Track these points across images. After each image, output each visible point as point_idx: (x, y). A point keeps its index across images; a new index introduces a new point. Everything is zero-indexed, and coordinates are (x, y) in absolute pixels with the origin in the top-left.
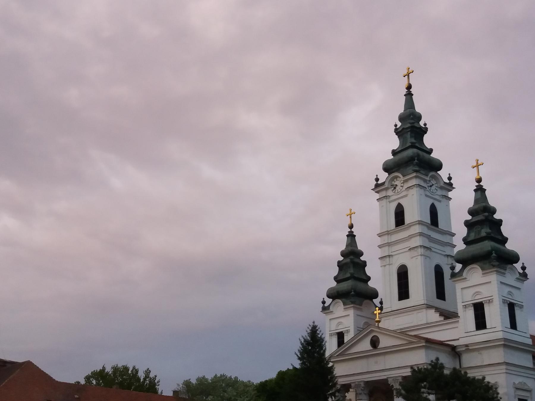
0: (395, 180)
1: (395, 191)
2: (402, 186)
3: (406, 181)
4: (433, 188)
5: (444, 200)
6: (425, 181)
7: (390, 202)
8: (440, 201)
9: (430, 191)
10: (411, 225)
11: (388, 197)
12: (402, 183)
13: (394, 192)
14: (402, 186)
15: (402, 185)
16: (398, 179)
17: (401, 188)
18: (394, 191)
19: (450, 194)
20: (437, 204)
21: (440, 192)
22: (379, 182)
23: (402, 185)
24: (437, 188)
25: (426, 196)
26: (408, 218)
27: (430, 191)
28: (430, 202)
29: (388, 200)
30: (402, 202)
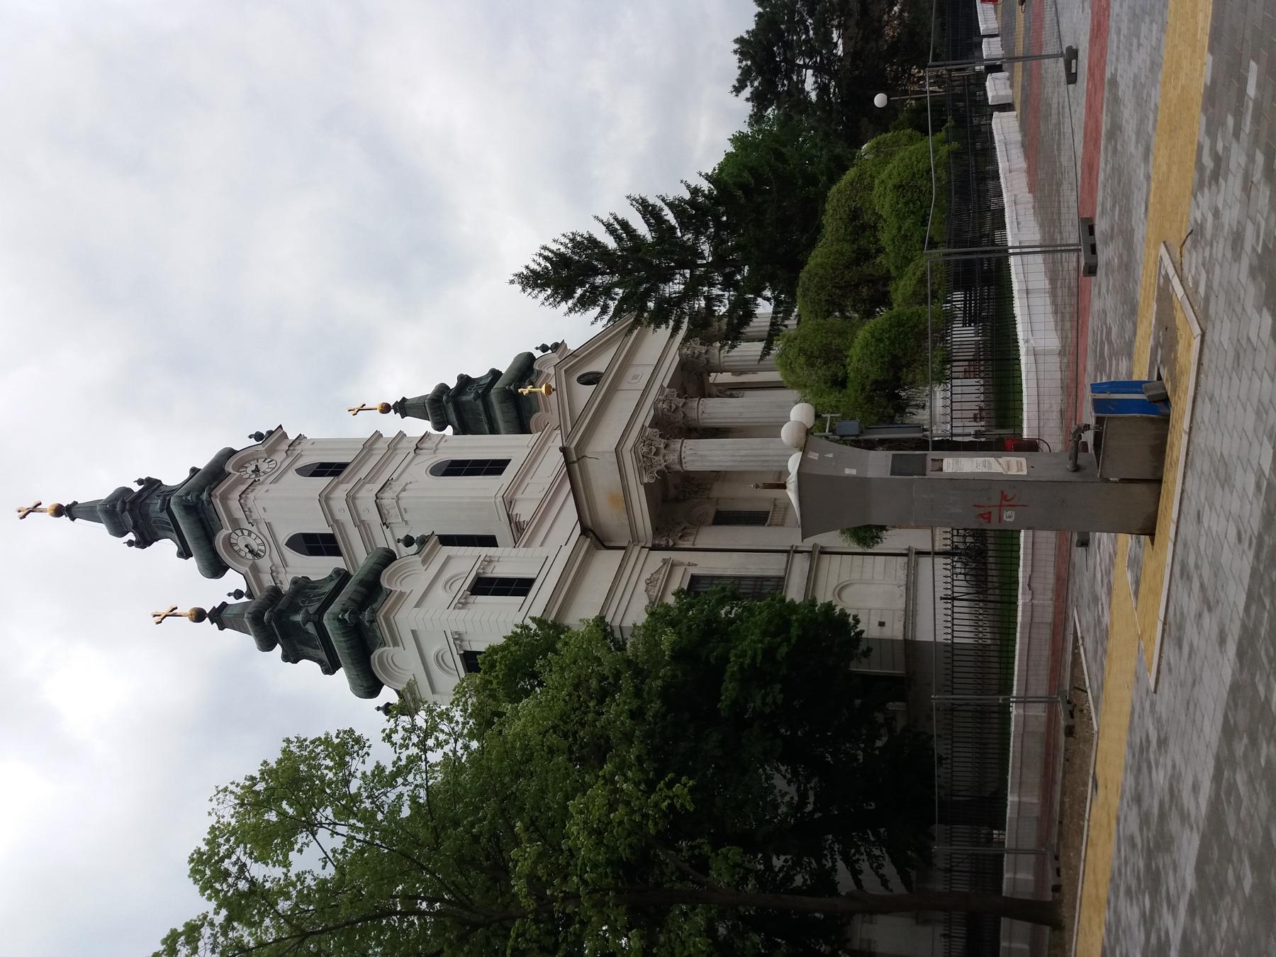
0: (236, 548)
1: (260, 550)
2: (249, 535)
3: (235, 523)
4: (264, 467)
5: (299, 448)
6: (240, 481)
7: (285, 564)
8: (299, 456)
11: (273, 568)
13: (263, 554)
15: (246, 533)
16: (233, 541)
17: (253, 535)
18: (263, 554)
19: (292, 436)
21: (279, 457)
22: (244, 589)
23: (246, 533)
24: (269, 460)
25: (275, 481)
26: (321, 527)
28: (292, 475)
30: (283, 537)
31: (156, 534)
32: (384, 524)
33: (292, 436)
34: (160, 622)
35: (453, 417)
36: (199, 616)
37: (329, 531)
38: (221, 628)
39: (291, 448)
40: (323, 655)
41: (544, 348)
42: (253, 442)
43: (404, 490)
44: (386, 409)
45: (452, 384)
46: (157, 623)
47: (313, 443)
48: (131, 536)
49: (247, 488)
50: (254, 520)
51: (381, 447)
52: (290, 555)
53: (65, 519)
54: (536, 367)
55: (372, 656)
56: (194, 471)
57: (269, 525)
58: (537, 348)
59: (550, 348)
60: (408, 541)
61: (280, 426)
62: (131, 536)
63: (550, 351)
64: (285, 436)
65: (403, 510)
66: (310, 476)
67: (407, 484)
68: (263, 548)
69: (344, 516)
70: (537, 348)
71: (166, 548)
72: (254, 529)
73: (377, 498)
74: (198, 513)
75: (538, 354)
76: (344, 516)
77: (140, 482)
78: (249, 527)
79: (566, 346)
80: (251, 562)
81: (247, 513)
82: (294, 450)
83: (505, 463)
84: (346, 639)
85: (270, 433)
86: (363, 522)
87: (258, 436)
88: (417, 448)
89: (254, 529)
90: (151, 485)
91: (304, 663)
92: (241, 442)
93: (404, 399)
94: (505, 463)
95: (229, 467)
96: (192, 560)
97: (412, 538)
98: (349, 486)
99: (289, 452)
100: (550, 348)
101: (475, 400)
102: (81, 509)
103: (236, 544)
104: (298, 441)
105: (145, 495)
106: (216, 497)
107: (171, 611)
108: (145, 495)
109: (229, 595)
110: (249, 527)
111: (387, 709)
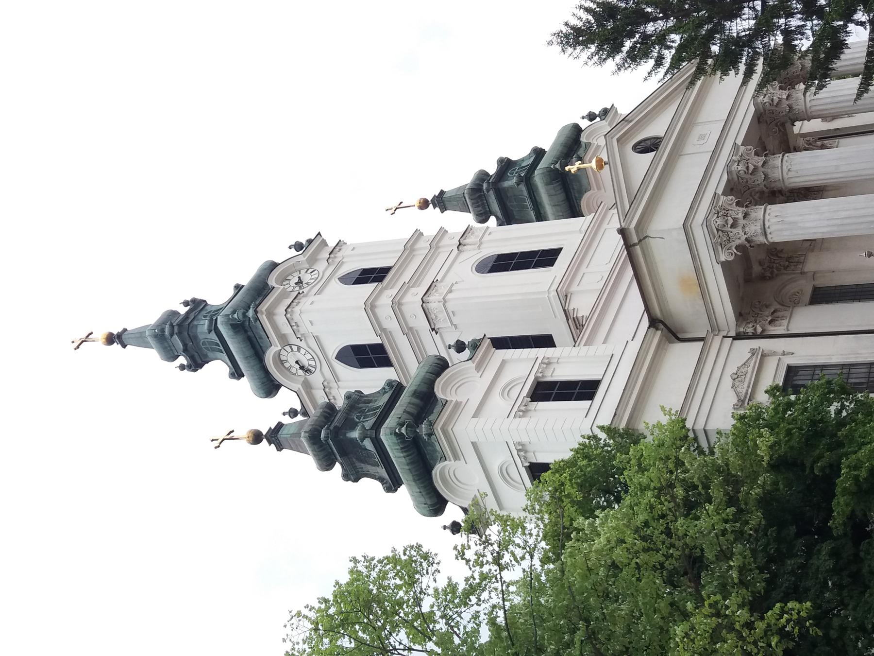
1: (311, 366)
2: (299, 351)
4: (306, 278)
5: (340, 255)
6: (284, 295)
7: (337, 379)
8: (341, 264)
9: (312, 283)
10: (381, 330)
11: (325, 384)
12: (292, 350)
13: (314, 369)
14: (299, 351)
15: (295, 348)
16: (283, 358)
20: (344, 270)
23: (295, 348)
26: (369, 338)
27: (312, 283)
28: (336, 286)
29: (333, 384)
30: (333, 350)
31: (206, 356)
32: (433, 329)
33: (332, 244)
35: (495, 206)
36: (257, 438)
37: (377, 341)
38: (280, 448)
39: (332, 256)
40: (383, 472)
41: (591, 117)
42: (293, 252)
43: (450, 291)
44: (424, 204)
46: (216, 448)
47: (353, 249)
48: (182, 360)
49: (292, 302)
50: (302, 335)
51: (423, 246)
52: (341, 368)
53: (116, 346)
54: (583, 139)
55: (433, 472)
56: (238, 288)
57: (317, 339)
58: (583, 118)
59: (599, 116)
60: (460, 347)
61: (319, 234)
62: (182, 360)
63: (598, 119)
64: (324, 243)
65: (451, 314)
66: (353, 284)
67: (453, 285)
68: (313, 363)
69: (392, 324)
70: (583, 118)
71: (218, 368)
72: (302, 344)
73: (423, 302)
74: (246, 331)
75: (584, 124)
76: (392, 324)
77: (186, 304)
78: (298, 342)
79: (616, 111)
80: (302, 379)
81: (295, 328)
82: (335, 257)
83: (556, 252)
84: (405, 454)
85: (310, 242)
86: (411, 329)
87: (298, 246)
88: (460, 244)
89: (302, 344)
90: (197, 306)
92: (282, 254)
93: (442, 193)
94: (556, 252)
95: (272, 281)
96: (245, 380)
97: (463, 343)
98: (394, 292)
99: (330, 260)
100: (599, 116)
101: (518, 185)
102: (133, 336)
103: (287, 361)
104: (338, 248)
105: (192, 316)
106: (262, 313)
108: (192, 316)
109: (284, 414)
110: (298, 342)
111: (455, 528)
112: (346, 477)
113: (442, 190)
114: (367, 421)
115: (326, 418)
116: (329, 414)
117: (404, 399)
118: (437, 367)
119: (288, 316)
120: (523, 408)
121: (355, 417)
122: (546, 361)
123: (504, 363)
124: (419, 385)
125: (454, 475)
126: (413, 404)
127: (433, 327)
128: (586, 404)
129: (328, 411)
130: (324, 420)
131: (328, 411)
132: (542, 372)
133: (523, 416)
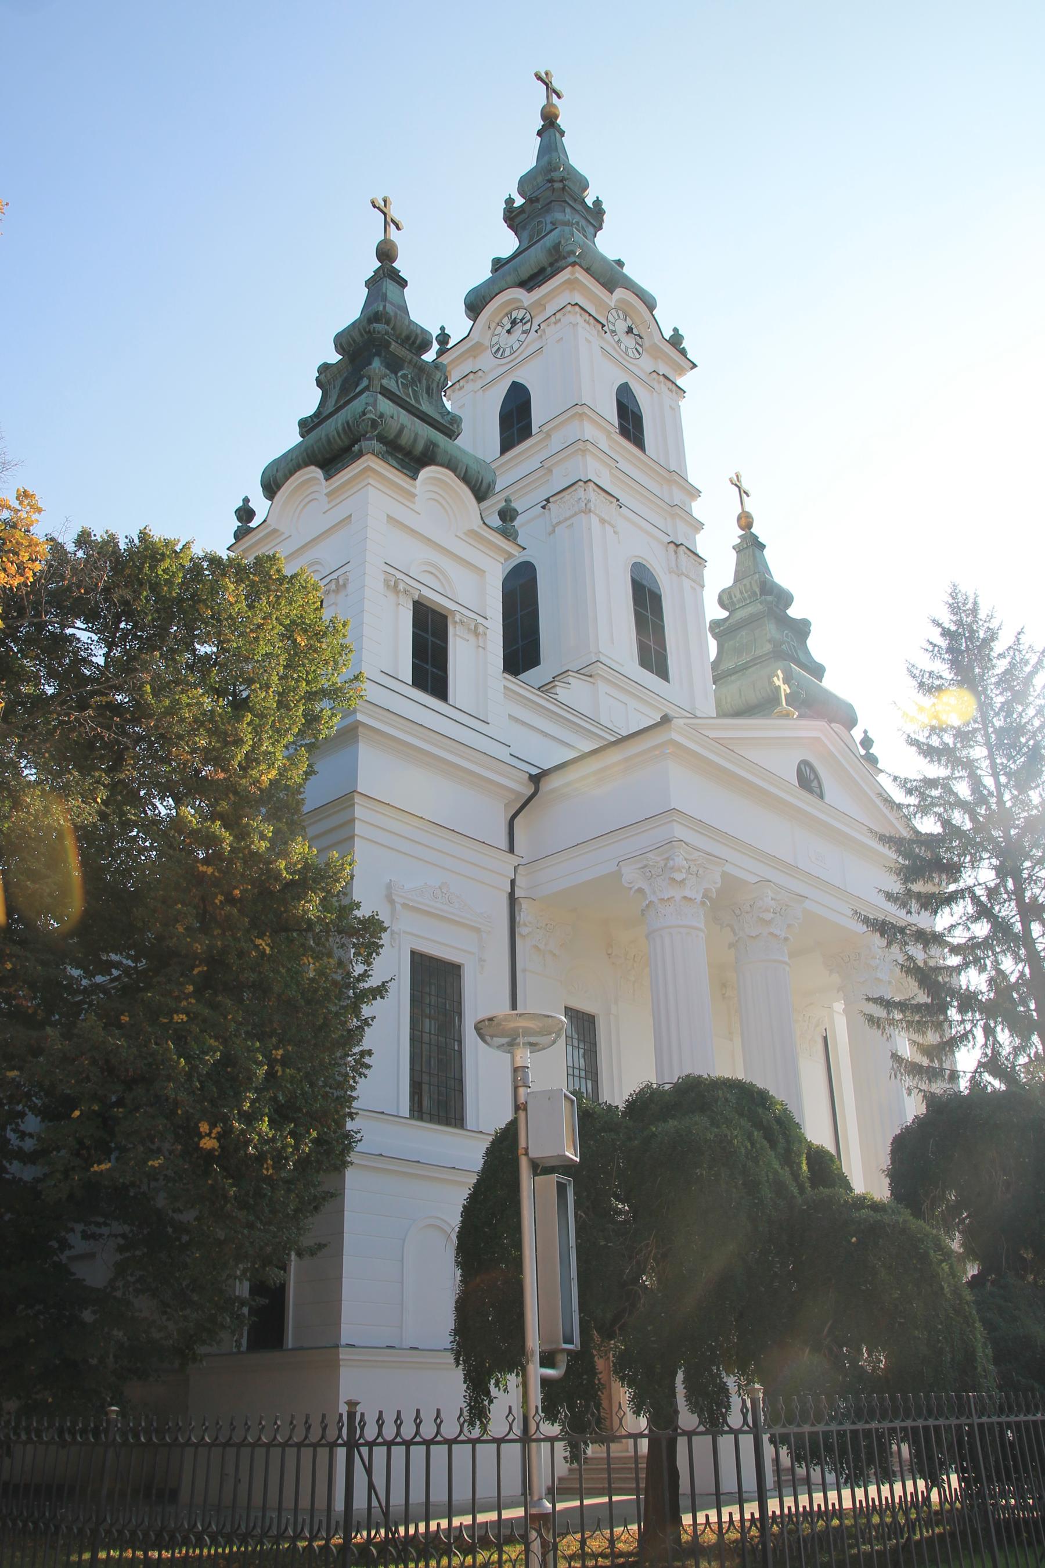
2: (524, 332)
13: (499, 356)
24: (640, 350)
26: (537, 417)
29: (480, 383)
31: (524, 228)
32: (548, 500)
34: (374, 206)
35: (741, 614)
39: (662, 378)
42: (668, 334)
43: (603, 521)
44: (745, 521)
45: (794, 612)
47: (673, 409)
48: (519, 201)
49: (590, 315)
50: (544, 331)
51: (678, 497)
53: (539, 123)
56: (620, 263)
60: (507, 515)
61: (695, 366)
62: (519, 201)
64: (681, 371)
65: (569, 522)
67: (613, 527)
68: (507, 353)
69: (556, 443)
71: (508, 243)
73: (585, 482)
74: (551, 265)
76: (556, 443)
77: (598, 203)
80: (487, 343)
81: (553, 319)
82: (659, 382)
83: (662, 671)
85: (683, 352)
86: (550, 471)
87: (676, 340)
88: (677, 546)
90: (596, 216)
91: (316, 395)
92: (667, 320)
93: (762, 547)
94: (662, 671)
95: (620, 293)
97: (513, 519)
98: (604, 444)
99: (654, 375)
101: (769, 641)
102: (553, 137)
104: (674, 388)
105: (579, 207)
107: (392, 221)
108: (579, 207)
110: (535, 327)
112: (324, 368)
113: (765, 546)
114: (398, 386)
115: (408, 338)
116: (414, 342)
117: (426, 432)
118: (477, 481)
119: (569, 307)
120: (401, 586)
121: (404, 372)
122: (481, 629)
123: (480, 572)
124: (446, 452)
125: (313, 500)
126: (415, 440)
127: (551, 500)
128: (408, 676)
129: (418, 342)
130: (404, 334)
131: (418, 342)
132: (462, 622)
133: (388, 586)
